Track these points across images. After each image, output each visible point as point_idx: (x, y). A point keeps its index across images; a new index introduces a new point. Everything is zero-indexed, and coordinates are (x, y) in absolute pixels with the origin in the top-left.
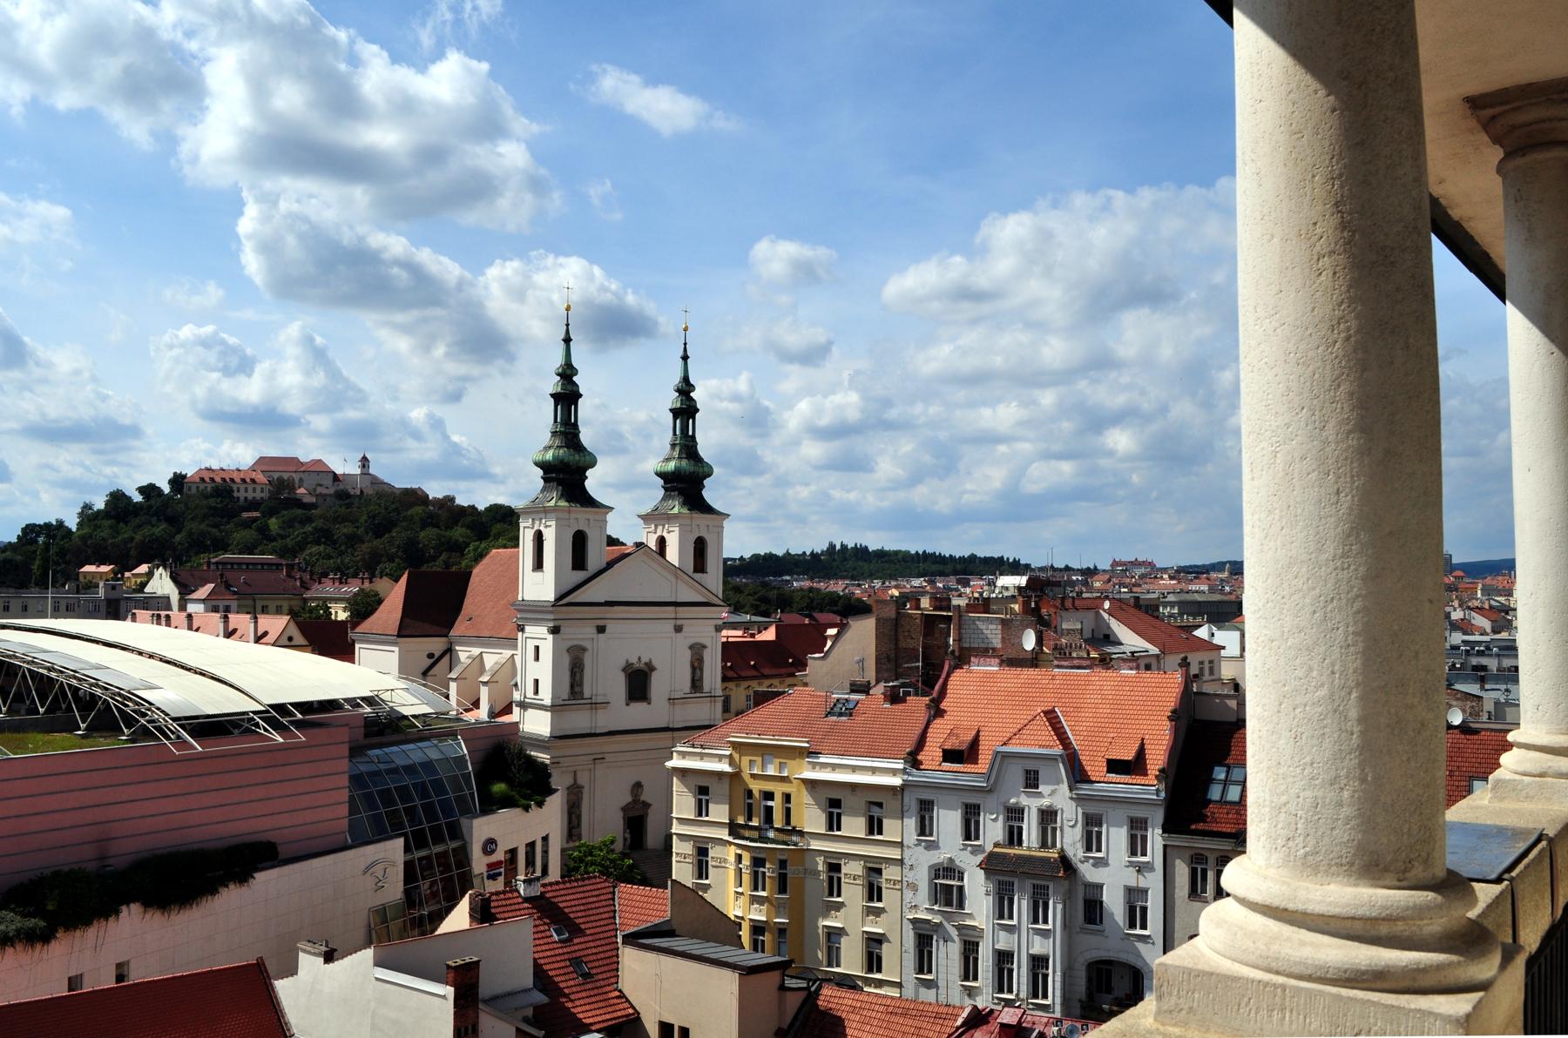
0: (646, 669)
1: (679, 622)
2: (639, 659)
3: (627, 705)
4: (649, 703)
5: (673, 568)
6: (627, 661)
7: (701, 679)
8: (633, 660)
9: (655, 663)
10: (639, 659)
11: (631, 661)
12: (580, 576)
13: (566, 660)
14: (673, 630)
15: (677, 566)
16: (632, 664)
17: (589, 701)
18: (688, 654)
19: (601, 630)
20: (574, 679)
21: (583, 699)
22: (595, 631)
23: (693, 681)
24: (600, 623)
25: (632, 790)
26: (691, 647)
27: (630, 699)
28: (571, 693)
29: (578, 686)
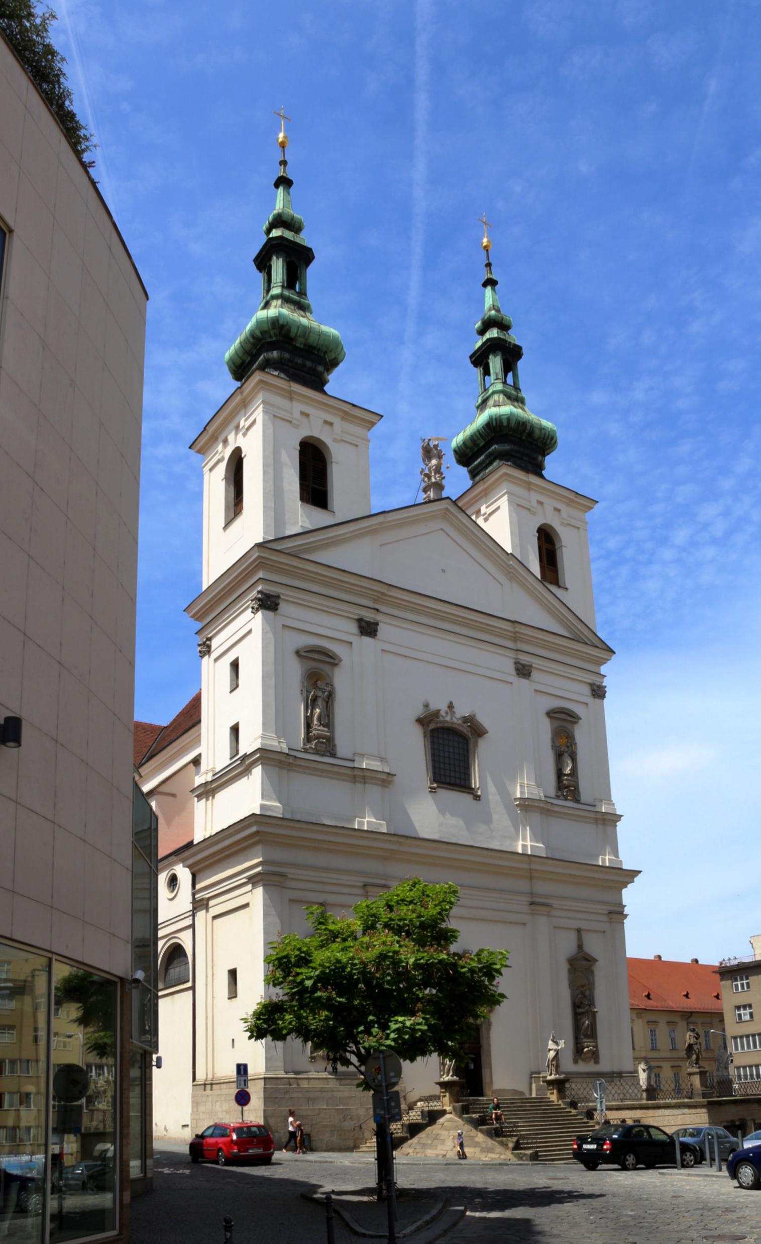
0: (465, 729)
1: (525, 659)
2: (451, 706)
5: (503, 557)
6: (426, 706)
8: (439, 704)
9: (483, 720)
10: (451, 706)
11: (434, 707)
13: (295, 671)
14: (514, 672)
15: (509, 551)
16: (437, 713)
18: (545, 728)
19: (368, 629)
21: (333, 755)
22: (353, 628)
24: (369, 616)
26: (551, 714)
27: (435, 780)
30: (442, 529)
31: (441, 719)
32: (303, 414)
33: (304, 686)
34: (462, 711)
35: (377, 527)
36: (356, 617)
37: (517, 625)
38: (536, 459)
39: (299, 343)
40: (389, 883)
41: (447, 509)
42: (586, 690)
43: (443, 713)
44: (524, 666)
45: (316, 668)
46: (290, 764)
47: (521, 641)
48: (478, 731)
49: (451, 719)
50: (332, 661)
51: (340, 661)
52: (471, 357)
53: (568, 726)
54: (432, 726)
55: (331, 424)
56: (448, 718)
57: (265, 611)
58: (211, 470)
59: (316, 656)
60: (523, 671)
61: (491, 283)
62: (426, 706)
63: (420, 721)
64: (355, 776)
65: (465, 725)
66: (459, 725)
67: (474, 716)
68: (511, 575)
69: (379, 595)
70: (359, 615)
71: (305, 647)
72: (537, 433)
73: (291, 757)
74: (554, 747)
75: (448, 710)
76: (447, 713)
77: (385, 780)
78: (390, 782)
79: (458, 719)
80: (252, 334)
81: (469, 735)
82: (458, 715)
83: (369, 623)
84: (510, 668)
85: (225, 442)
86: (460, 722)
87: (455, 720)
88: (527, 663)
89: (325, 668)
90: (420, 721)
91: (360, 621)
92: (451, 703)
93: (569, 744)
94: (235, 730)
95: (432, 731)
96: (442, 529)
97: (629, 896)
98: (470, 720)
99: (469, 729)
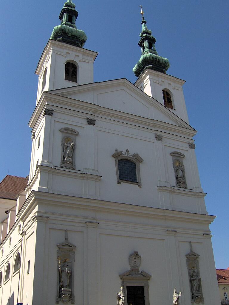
1: (159, 134)
2: (127, 151)
3: (119, 183)
4: (140, 186)
7: (183, 176)
9: (142, 155)
10: (127, 151)
11: (119, 150)
12: (70, 84)
13: (59, 137)
14: (155, 139)
16: (121, 153)
17: (81, 172)
19: (91, 122)
20: (66, 152)
21: (75, 169)
22: (85, 122)
23: (177, 178)
25: (129, 259)
28: (63, 163)
29: (69, 157)
30: (123, 89)
31: (123, 155)
32: (67, 53)
33: (62, 143)
34: (131, 153)
35: (95, 87)
36: (86, 118)
37: (154, 121)
38: (162, 70)
39: (70, 35)
40: (98, 222)
41: (124, 82)
42: (187, 146)
43: (123, 153)
44: (159, 136)
45: (68, 136)
46: (54, 172)
47: (157, 127)
48: (141, 161)
49: (128, 155)
50: (75, 133)
51: (79, 134)
52: (138, 44)
53: (180, 159)
54: (119, 158)
55: (79, 56)
56: (126, 155)
57: (47, 116)
58: (40, 78)
59: (68, 132)
60: (159, 138)
61: (145, 23)
62: (117, 150)
63: (113, 156)
64: (83, 177)
65: (134, 158)
66: (131, 158)
67: (138, 154)
68: (152, 104)
69: (96, 110)
70: (87, 117)
71: (63, 128)
72: (161, 61)
73: (53, 169)
74: (174, 167)
75: (126, 152)
76: (126, 153)
77: (98, 178)
78: (100, 180)
79: (131, 156)
80: (54, 35)
81: (136, 161)
82: (130, 155)
83: (91, 120)
84: (153, 137)
85: (44, 68)
86: (131, 157)
87: (129, 156)
88: (160, 135)
89: (73, 137)
90: (113, 156)
91: (88, 119)
92: (127, 149)
93: (180, 166)
94: (38, 162)
95: (119, 161)
96: (123, 89)
97: (212, 227)
98: (136, 156)
99: (135, 159)
